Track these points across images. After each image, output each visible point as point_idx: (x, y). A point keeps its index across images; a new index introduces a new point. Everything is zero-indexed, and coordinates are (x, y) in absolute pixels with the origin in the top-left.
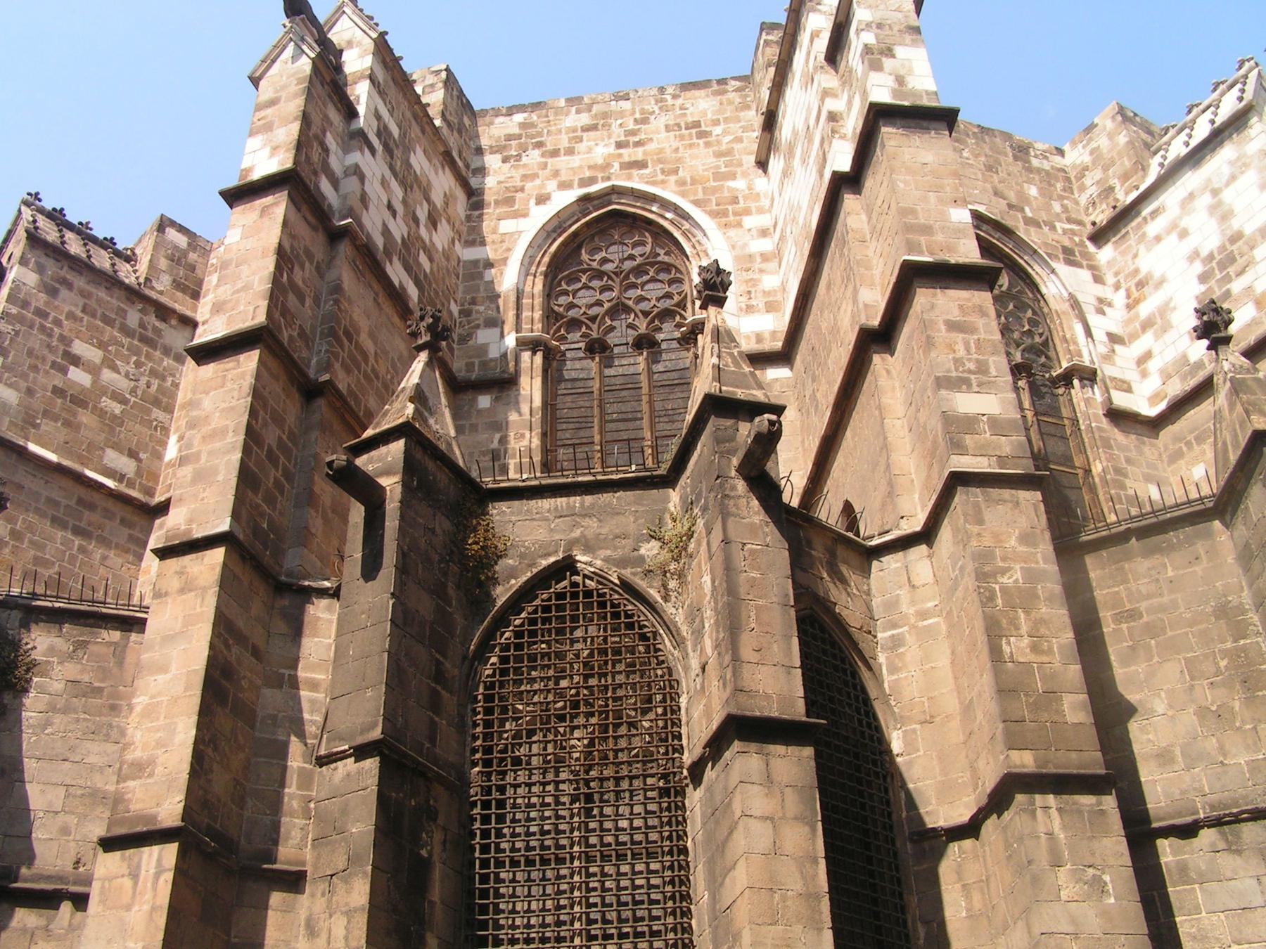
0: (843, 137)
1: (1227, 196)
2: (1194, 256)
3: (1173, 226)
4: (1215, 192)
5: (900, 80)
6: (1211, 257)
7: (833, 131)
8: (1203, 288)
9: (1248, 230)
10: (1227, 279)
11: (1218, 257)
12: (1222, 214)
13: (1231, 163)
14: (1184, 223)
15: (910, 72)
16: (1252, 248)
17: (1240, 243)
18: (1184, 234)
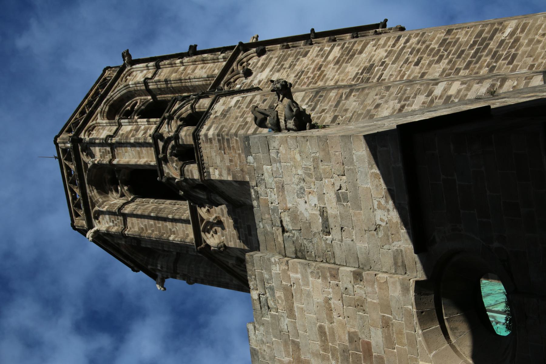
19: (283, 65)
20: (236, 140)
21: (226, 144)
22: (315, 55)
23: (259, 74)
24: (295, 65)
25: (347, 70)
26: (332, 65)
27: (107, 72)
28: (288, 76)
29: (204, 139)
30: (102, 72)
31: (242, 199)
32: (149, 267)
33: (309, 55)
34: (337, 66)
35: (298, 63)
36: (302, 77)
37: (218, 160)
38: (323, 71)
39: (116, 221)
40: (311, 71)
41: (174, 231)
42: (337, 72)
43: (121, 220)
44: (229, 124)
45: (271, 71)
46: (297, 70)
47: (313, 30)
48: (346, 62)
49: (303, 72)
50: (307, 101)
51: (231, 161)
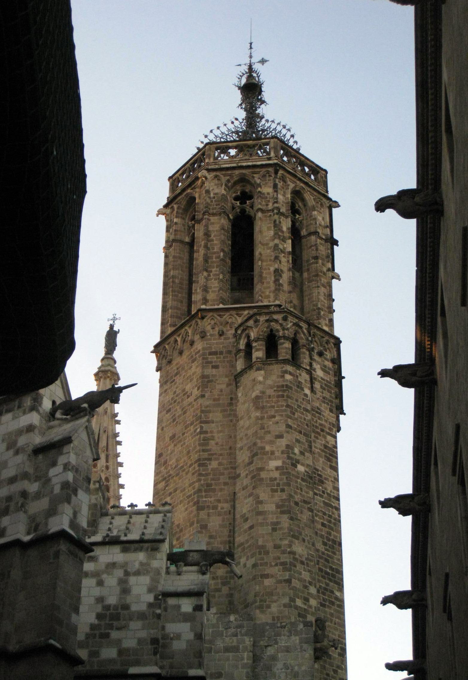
0: (26, 512)
1: (132, 580)
2: (100, 600)
3: (96, 574)
4: (127, 573)
5: (75, 514)
6: (107, 608)
7: (23, 506)
8: (96, 622)
9: (134, 608)
10: (111, 627)
11: (112, 611)
12: (125, 591)
13: (141, 564)
14: (104, 576)
15: (80, 509)
16: (131, 619)
17: (125, 612)
18: (100, 583)
19: (324, 389)
20: (282, 406)
21: (280, 393)
22: (330, 421)
23: (319, 366)
24: (324, 402)
25: (321, 459)
26: (323, 442)
27: (324, 173)
28: (318, 399)
29: (284, 369)
30: (324, 168)
31: (241, 388)
32: (175, 206)
33: (331, 414)
34: (322, 448)
35: (326, 405)
36: (317, 415)
37: (269, 382)
38: (319, 434)
39: (215, 201)
40: (320, 422)
41: (210, 276)
42: (320, 449)
43: (216, 208)
44: (294, 394)
45: (322, 378)
46: (321, 406)
47: (344, 378)
48: (325, 456)
49: (320, 414)
50: (307, 470)
51: (269, 397)
